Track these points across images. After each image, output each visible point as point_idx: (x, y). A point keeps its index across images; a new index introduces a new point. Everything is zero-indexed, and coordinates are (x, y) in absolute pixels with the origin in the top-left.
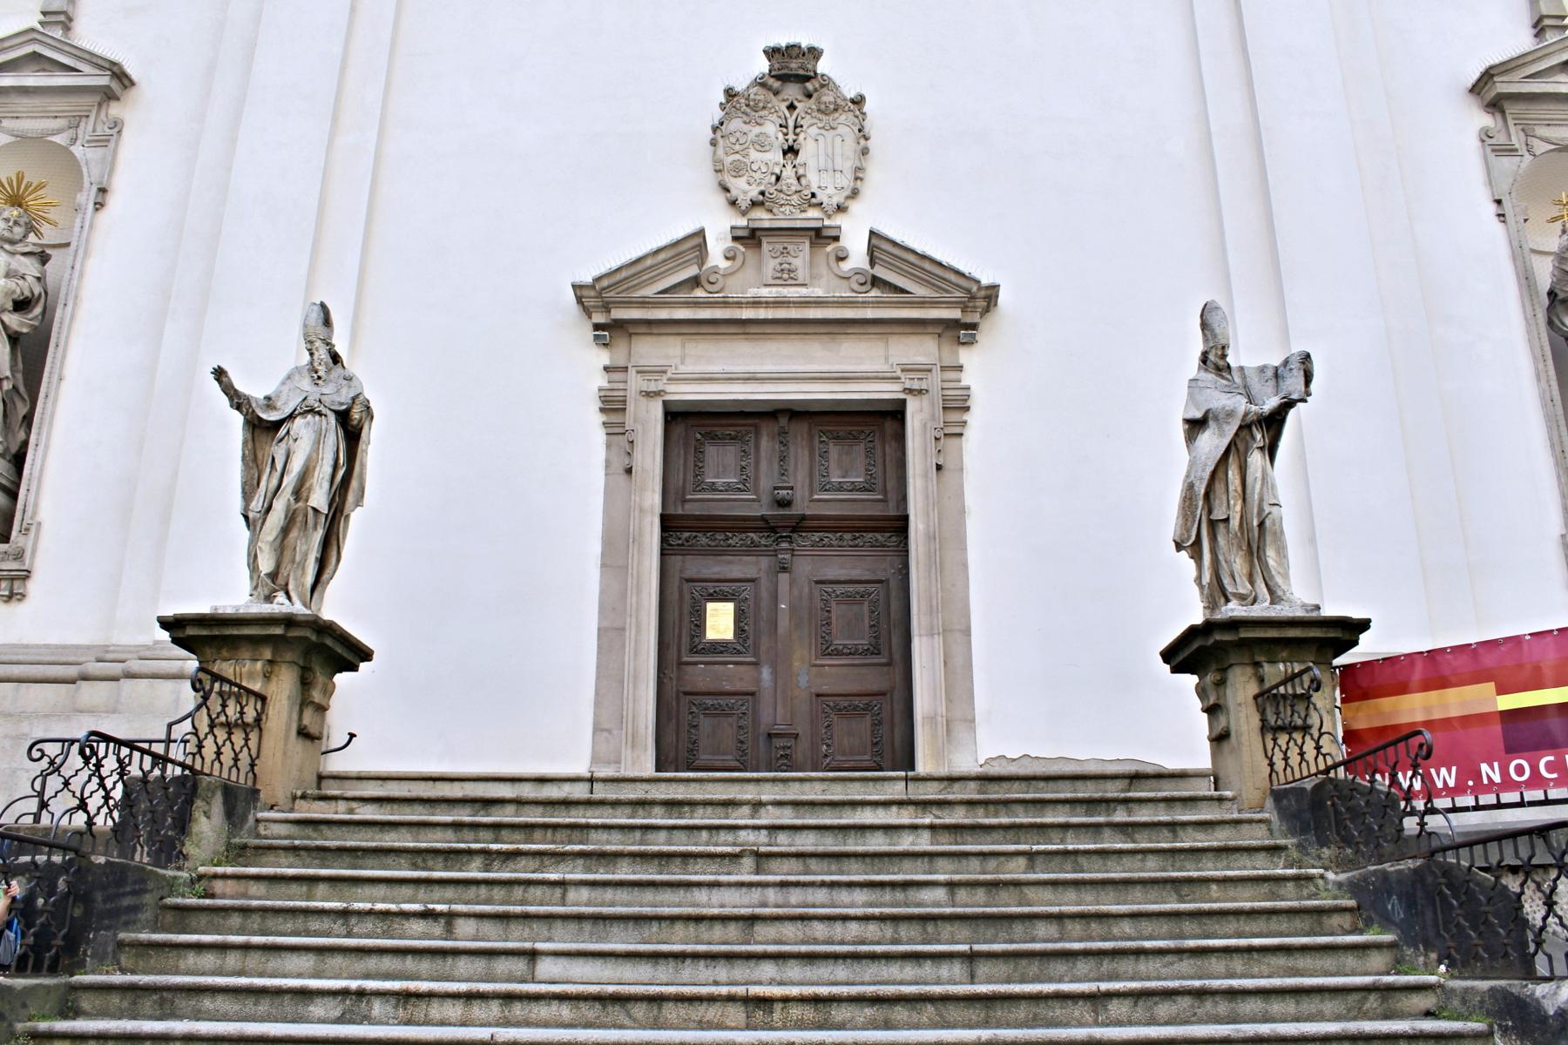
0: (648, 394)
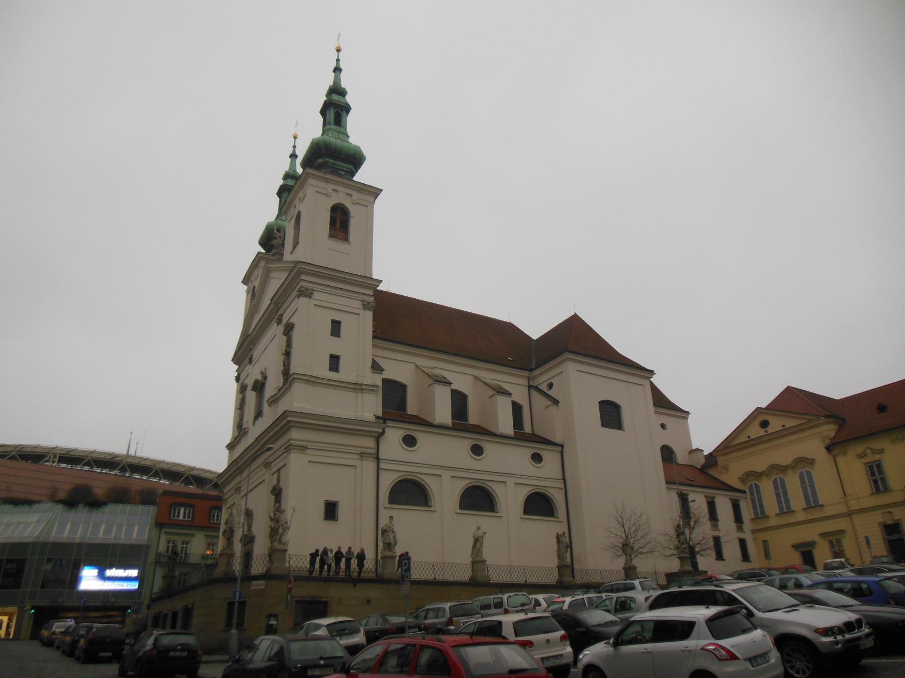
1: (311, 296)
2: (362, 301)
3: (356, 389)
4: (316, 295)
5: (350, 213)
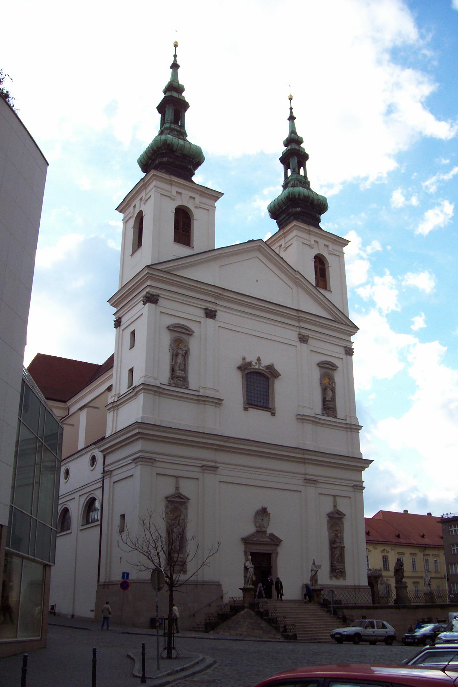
0: (249, 551)
1: (307, 342)
2: (345, 347)
3: (346, 428)
4: (310, 341)
5: (328, 263)
